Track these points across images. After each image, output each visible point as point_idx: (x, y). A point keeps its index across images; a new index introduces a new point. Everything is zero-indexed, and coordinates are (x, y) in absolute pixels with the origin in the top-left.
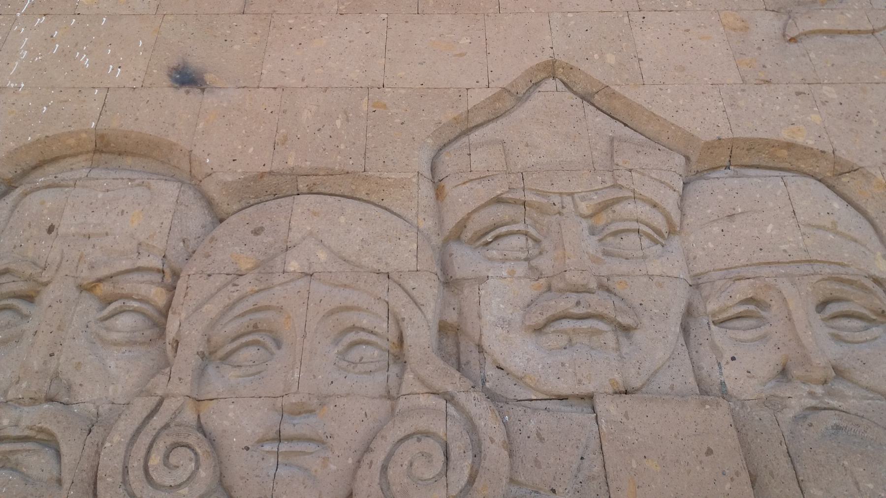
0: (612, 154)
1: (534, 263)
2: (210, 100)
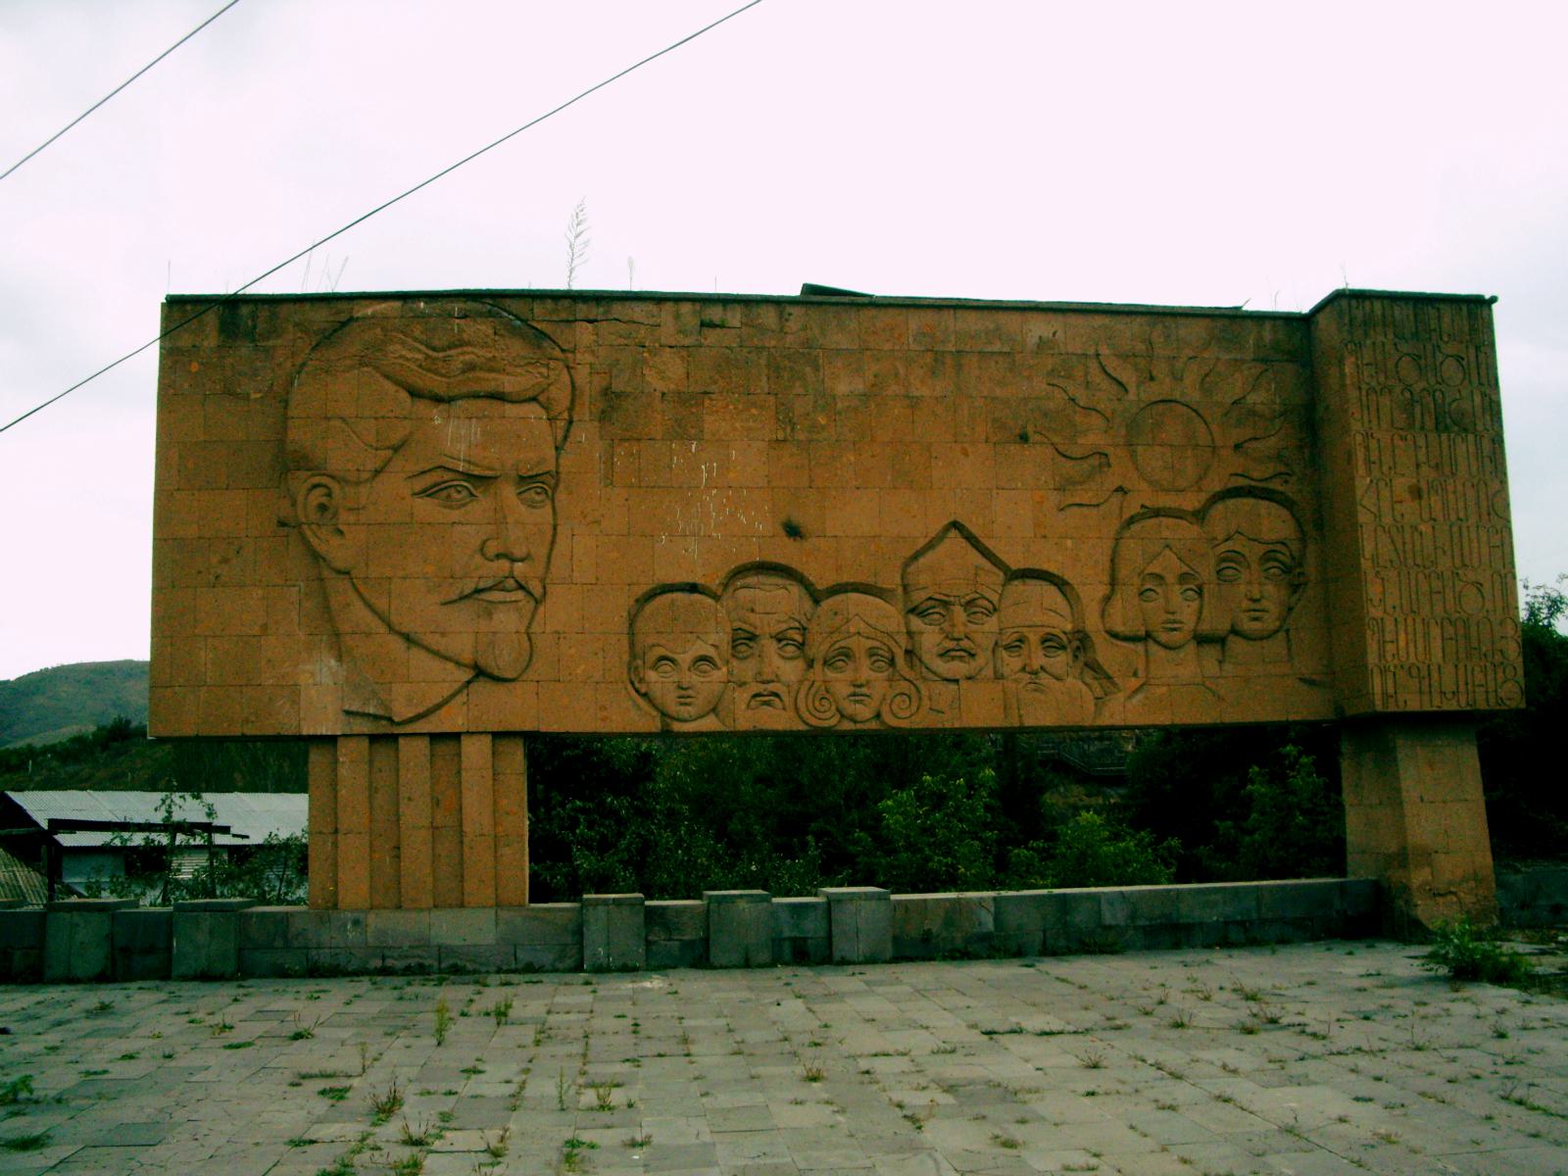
0: (976, 574)
2: (807, 545)
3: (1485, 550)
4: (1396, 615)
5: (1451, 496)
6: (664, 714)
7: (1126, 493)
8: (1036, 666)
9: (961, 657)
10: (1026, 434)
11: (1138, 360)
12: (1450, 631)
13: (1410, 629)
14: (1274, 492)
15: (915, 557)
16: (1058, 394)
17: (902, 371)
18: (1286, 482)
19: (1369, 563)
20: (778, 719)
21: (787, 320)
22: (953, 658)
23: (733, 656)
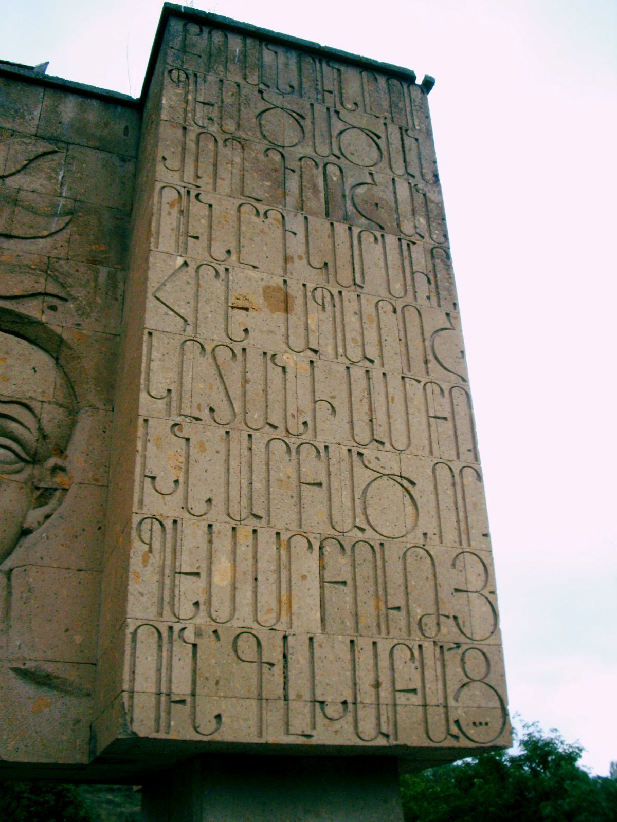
3: (418, 420)
4: (211, 518)
5: (352, 321)
12: (339, 566)
13: (245, 551)
18: (53, 308)
19: (161, 404)
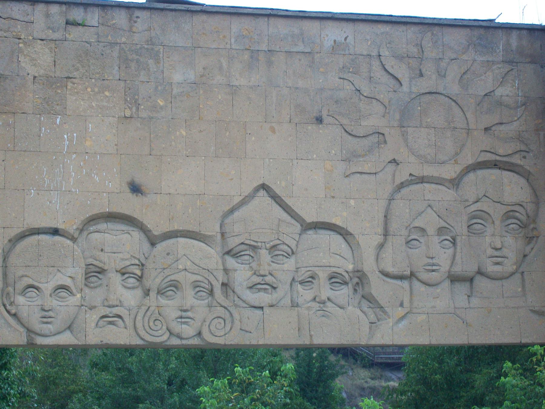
0: (279, 225)
1: (251, 265)
6: (29, 331)
7: (398, 164)
8: (324, 297)
9: (265, 289)
10: (321, 117)
11: (411, 61)
14: (512, 164)
15: (232, 211)
16: (349, 87)
17: (225, 65)
18: (524, 157)
20: (120, 336)
21: (135, 22)
22: (260, 290)
23: (86, 285)
